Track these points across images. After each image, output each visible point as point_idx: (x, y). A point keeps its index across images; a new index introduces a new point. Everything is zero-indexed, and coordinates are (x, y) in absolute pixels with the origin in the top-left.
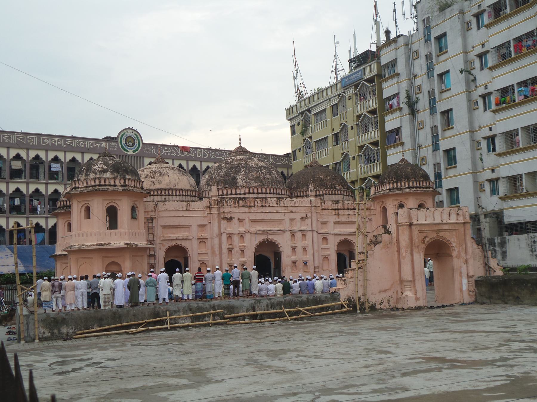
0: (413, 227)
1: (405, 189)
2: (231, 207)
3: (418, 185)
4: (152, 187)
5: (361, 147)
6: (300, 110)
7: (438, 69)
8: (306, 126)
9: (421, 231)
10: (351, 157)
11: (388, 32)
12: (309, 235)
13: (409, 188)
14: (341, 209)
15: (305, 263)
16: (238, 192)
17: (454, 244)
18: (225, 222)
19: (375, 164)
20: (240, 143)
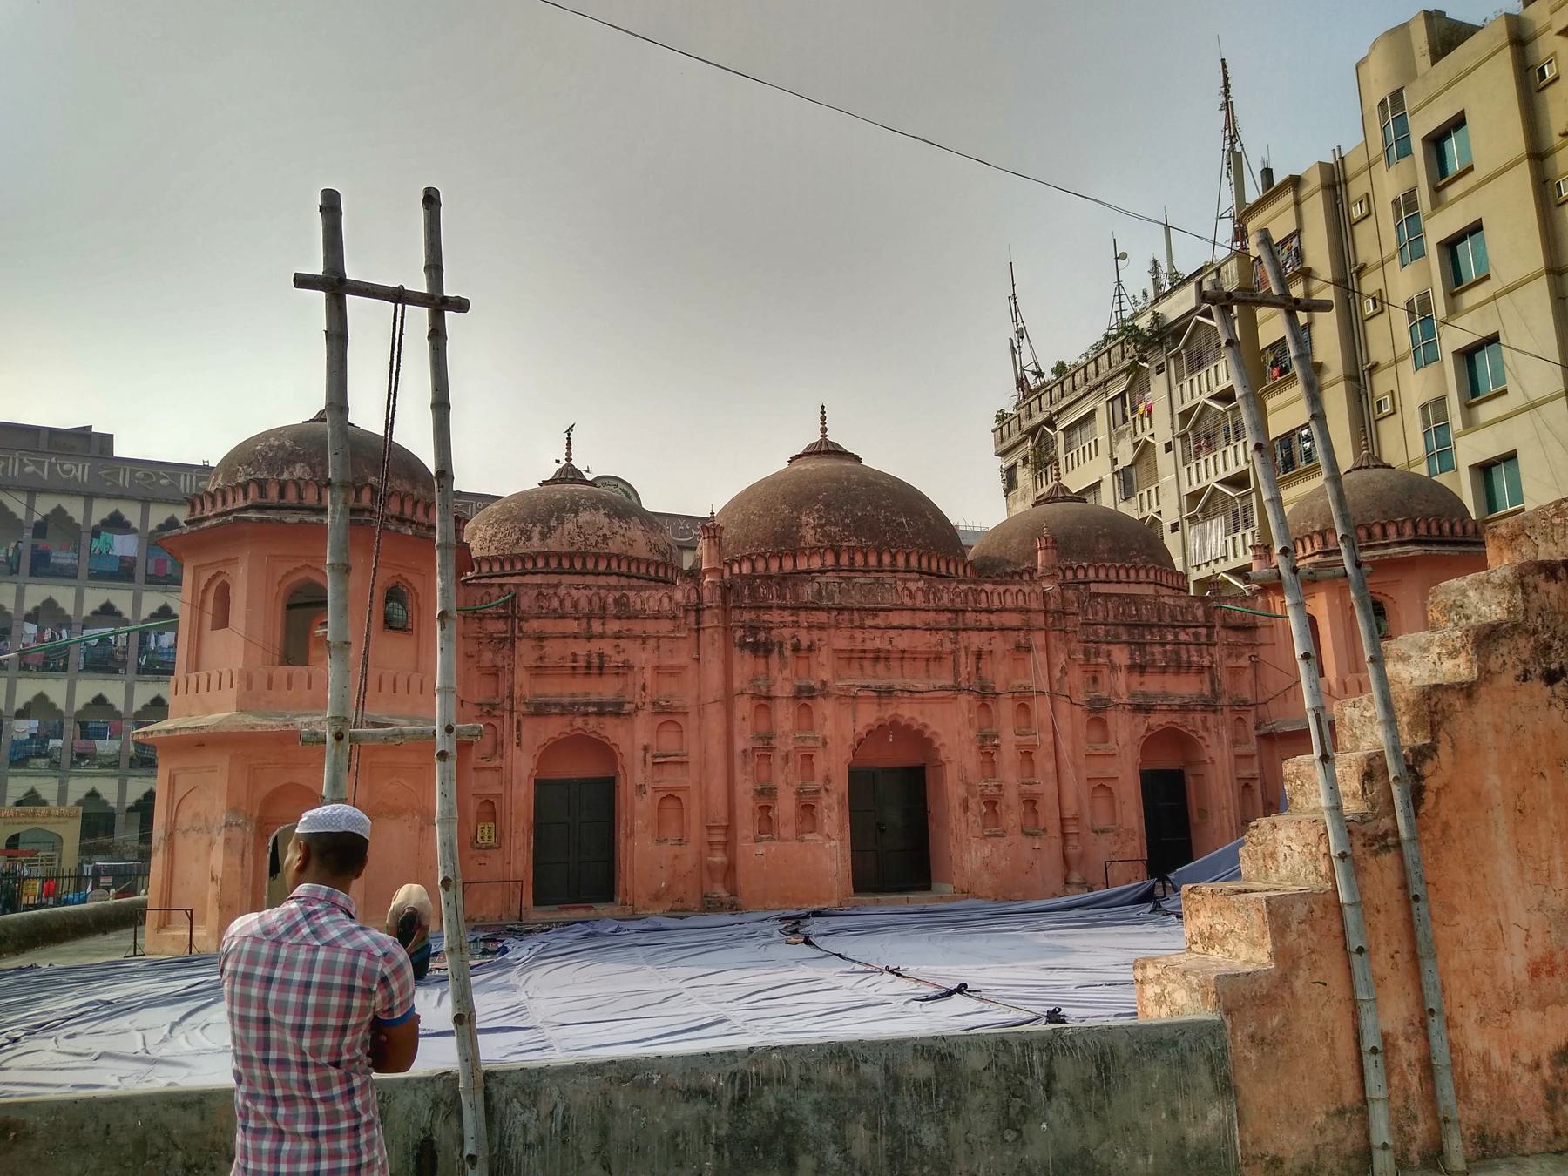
1: (1387, 546)
2: (770, 608)
3: (1435, 532)
4: (521, 549)
5: (1194, 497)
6: (1027, 424)
7: (1438, 228)
8: (1043, 461)
10: (1166, 526)
11: (1267, 173)
12: (1041, 708)
13: (1401, 544)
14: (1150, 626)
15: (1030, 802)
16: (802, 564)
18: (747, 653)
19: (1239, 536)
20: (824, 430)
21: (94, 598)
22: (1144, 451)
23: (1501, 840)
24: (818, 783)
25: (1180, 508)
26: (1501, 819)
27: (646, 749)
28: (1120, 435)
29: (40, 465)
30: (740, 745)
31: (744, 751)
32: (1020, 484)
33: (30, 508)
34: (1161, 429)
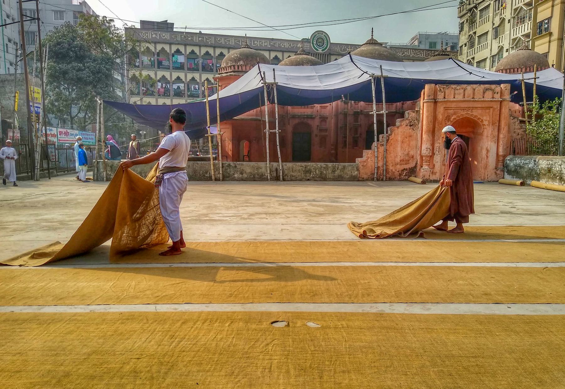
0: (439, 105)
6: (469, 7)
8: (472, 22)
9: (446, 109)
17: (486, 123)
20: (372, 35)
21: (175, 75)
22: (503, 21)
23: (399, 145)
24: (358, 135)
25: (509, 44)
26: (400, 143)
27: (318, 126)
28: (497, 14)
29: (156, 34)
30: (340, 125)
31: (341, 127)
32: (465, 29)
33: (155, 48)
34: (508, 14)
